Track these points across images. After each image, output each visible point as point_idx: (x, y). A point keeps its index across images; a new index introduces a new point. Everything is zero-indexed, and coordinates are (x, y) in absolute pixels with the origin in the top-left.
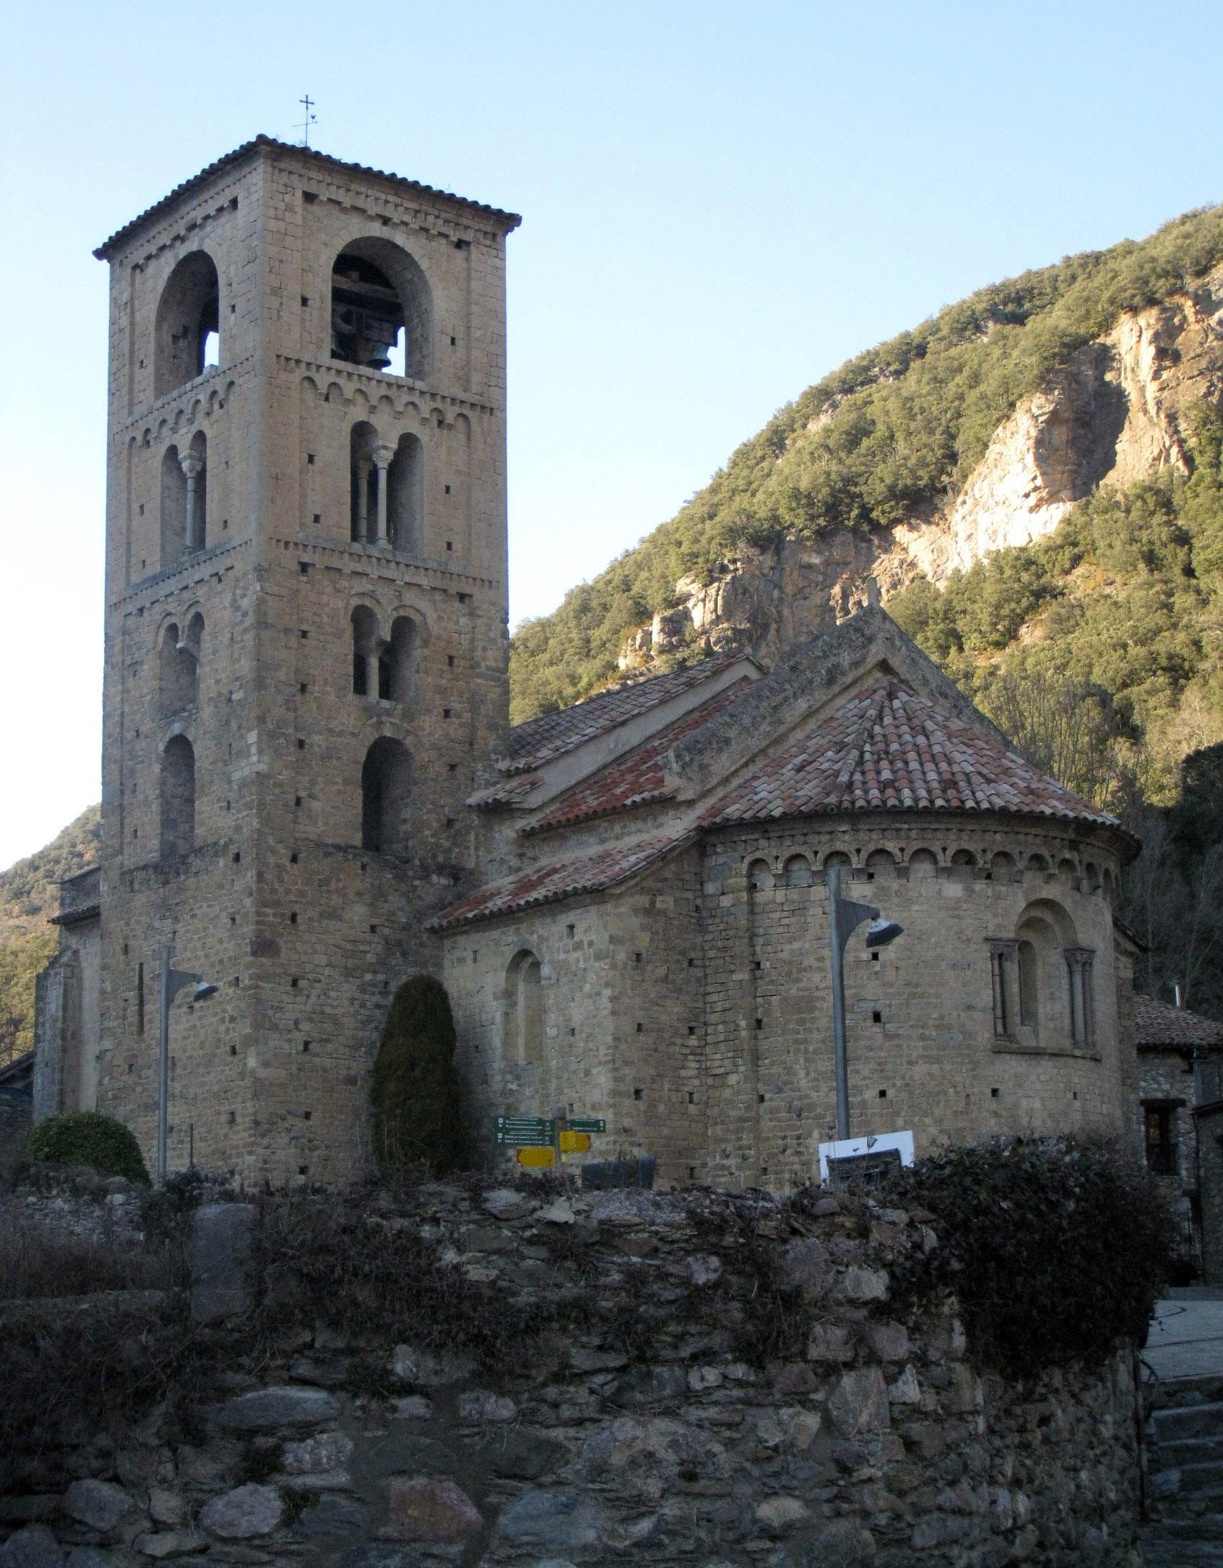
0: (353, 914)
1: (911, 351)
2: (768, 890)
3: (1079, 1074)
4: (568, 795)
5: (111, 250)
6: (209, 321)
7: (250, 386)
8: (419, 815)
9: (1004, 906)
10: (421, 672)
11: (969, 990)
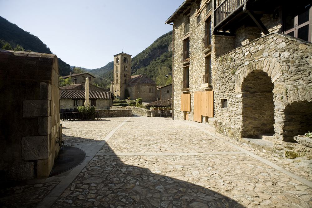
0: (124, 86)
1: (166, 35)
2: (141, 86)
3: (153, 94)
4: (133, 81)
5: (114, 56)
6: (118, 59)
7: (120, 64)
8: (127, 82)
9: (150, 87)
10: (127, 76)
11: (148, 90)
